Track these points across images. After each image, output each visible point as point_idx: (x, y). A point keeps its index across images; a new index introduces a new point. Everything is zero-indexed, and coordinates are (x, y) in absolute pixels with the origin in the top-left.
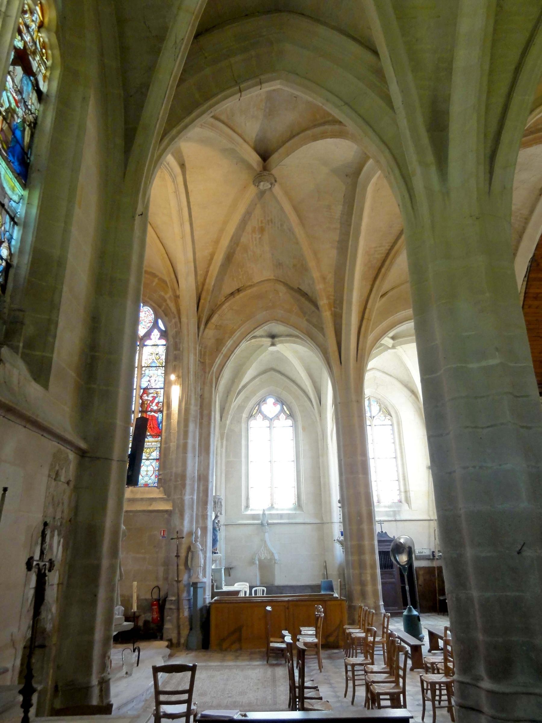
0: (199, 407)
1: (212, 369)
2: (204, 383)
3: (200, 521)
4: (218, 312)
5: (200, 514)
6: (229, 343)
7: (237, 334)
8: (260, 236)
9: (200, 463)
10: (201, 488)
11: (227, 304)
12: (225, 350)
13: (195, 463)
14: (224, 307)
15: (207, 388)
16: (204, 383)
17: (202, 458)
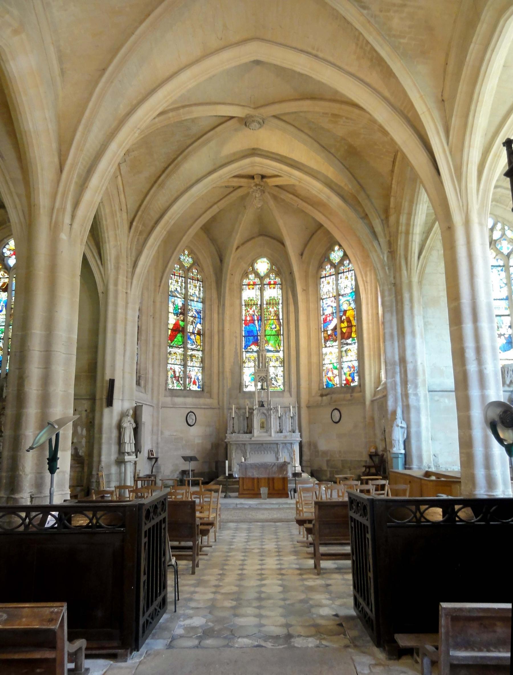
0: (394, 295)
1: (398, 252)
2: (395, 271)
3: (405, 400)
4: (392, 194)
5: (403, 393)
6: (403, 219)
7: (406, 204)
8: (344, 118)
9: (399, 346)
10: (402, 371)
11: (394, 182)
12: (402, 228)
13: (394, 349)
14: (393, 186)
15: (398, 275)
16: (395, 271)
17: (400, 342)
